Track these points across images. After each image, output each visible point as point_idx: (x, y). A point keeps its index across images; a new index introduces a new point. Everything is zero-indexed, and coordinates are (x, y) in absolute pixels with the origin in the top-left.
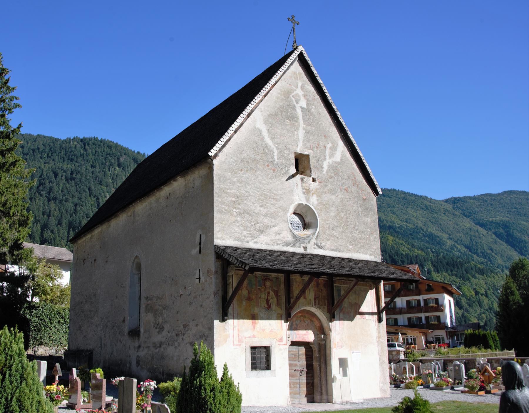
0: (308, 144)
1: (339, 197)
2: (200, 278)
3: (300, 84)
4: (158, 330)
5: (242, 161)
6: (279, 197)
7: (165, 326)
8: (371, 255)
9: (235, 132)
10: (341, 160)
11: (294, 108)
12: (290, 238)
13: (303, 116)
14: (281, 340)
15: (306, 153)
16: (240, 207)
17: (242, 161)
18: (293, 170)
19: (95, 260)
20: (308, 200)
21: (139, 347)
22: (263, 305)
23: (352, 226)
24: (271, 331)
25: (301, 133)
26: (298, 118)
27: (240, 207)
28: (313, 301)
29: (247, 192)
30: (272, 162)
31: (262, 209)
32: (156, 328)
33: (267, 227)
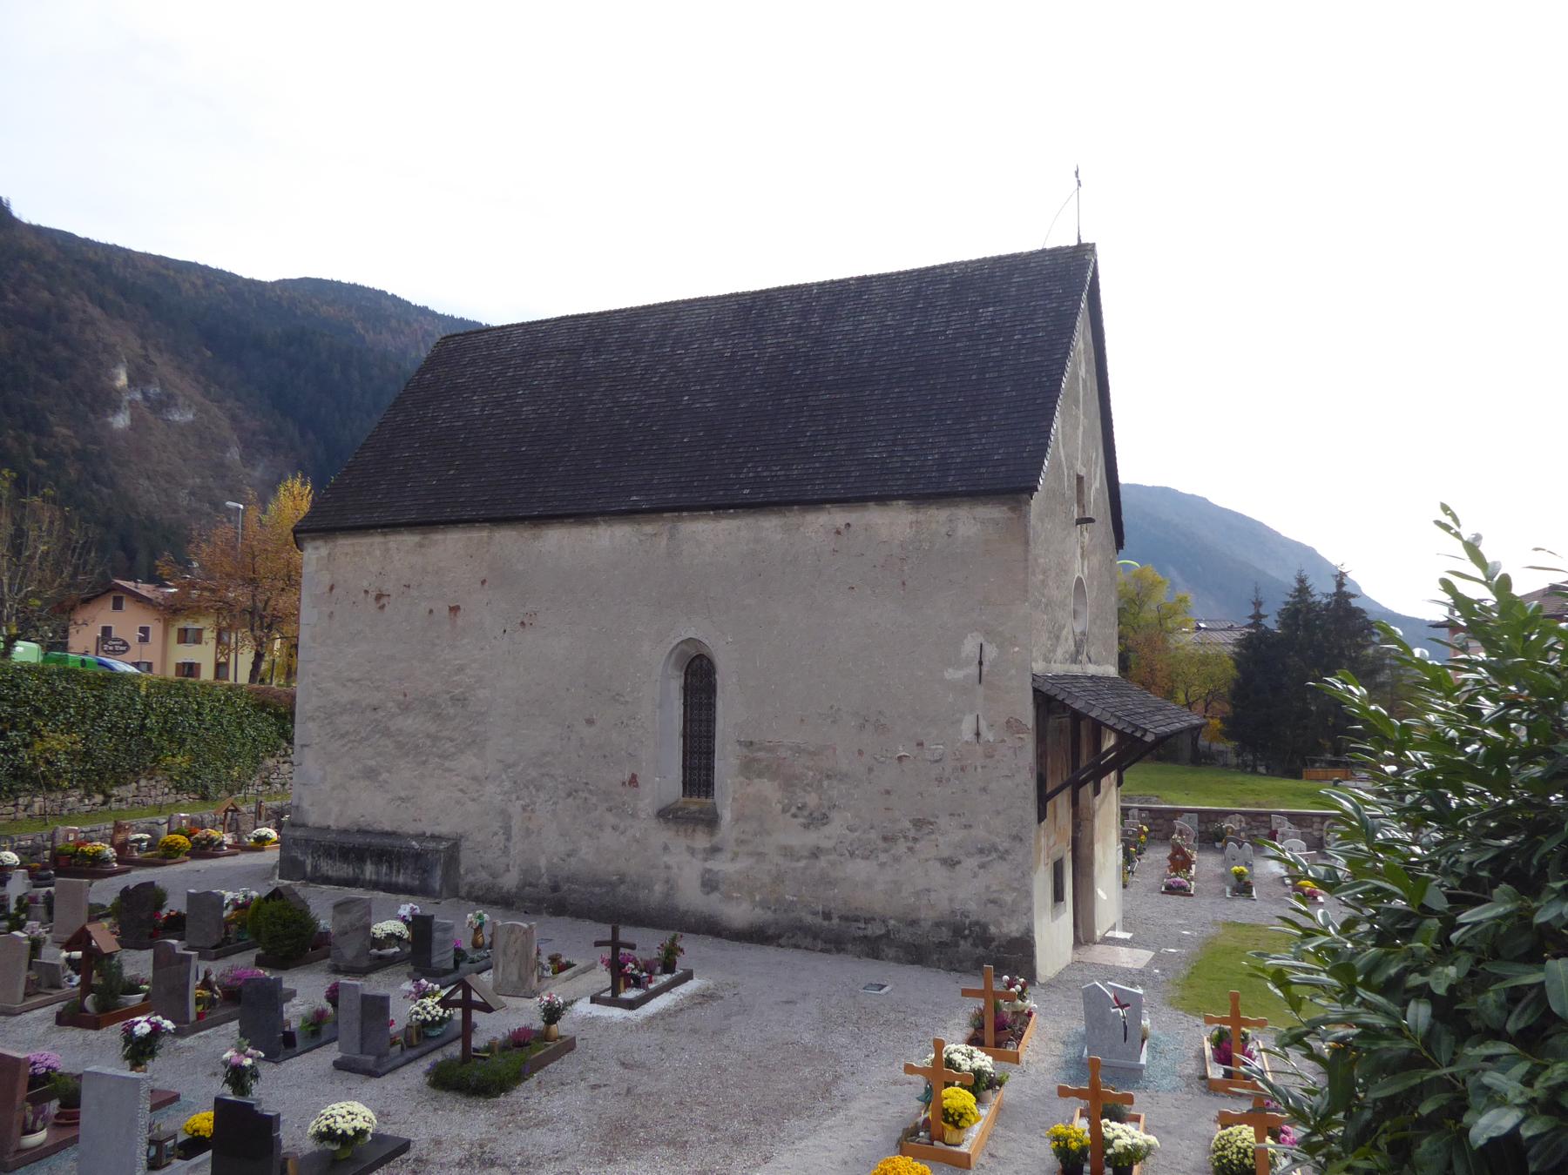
2: (978, 734)
4: (802, 820)
7: (833, 814)
19: (454, 610)
32: (794, 816)
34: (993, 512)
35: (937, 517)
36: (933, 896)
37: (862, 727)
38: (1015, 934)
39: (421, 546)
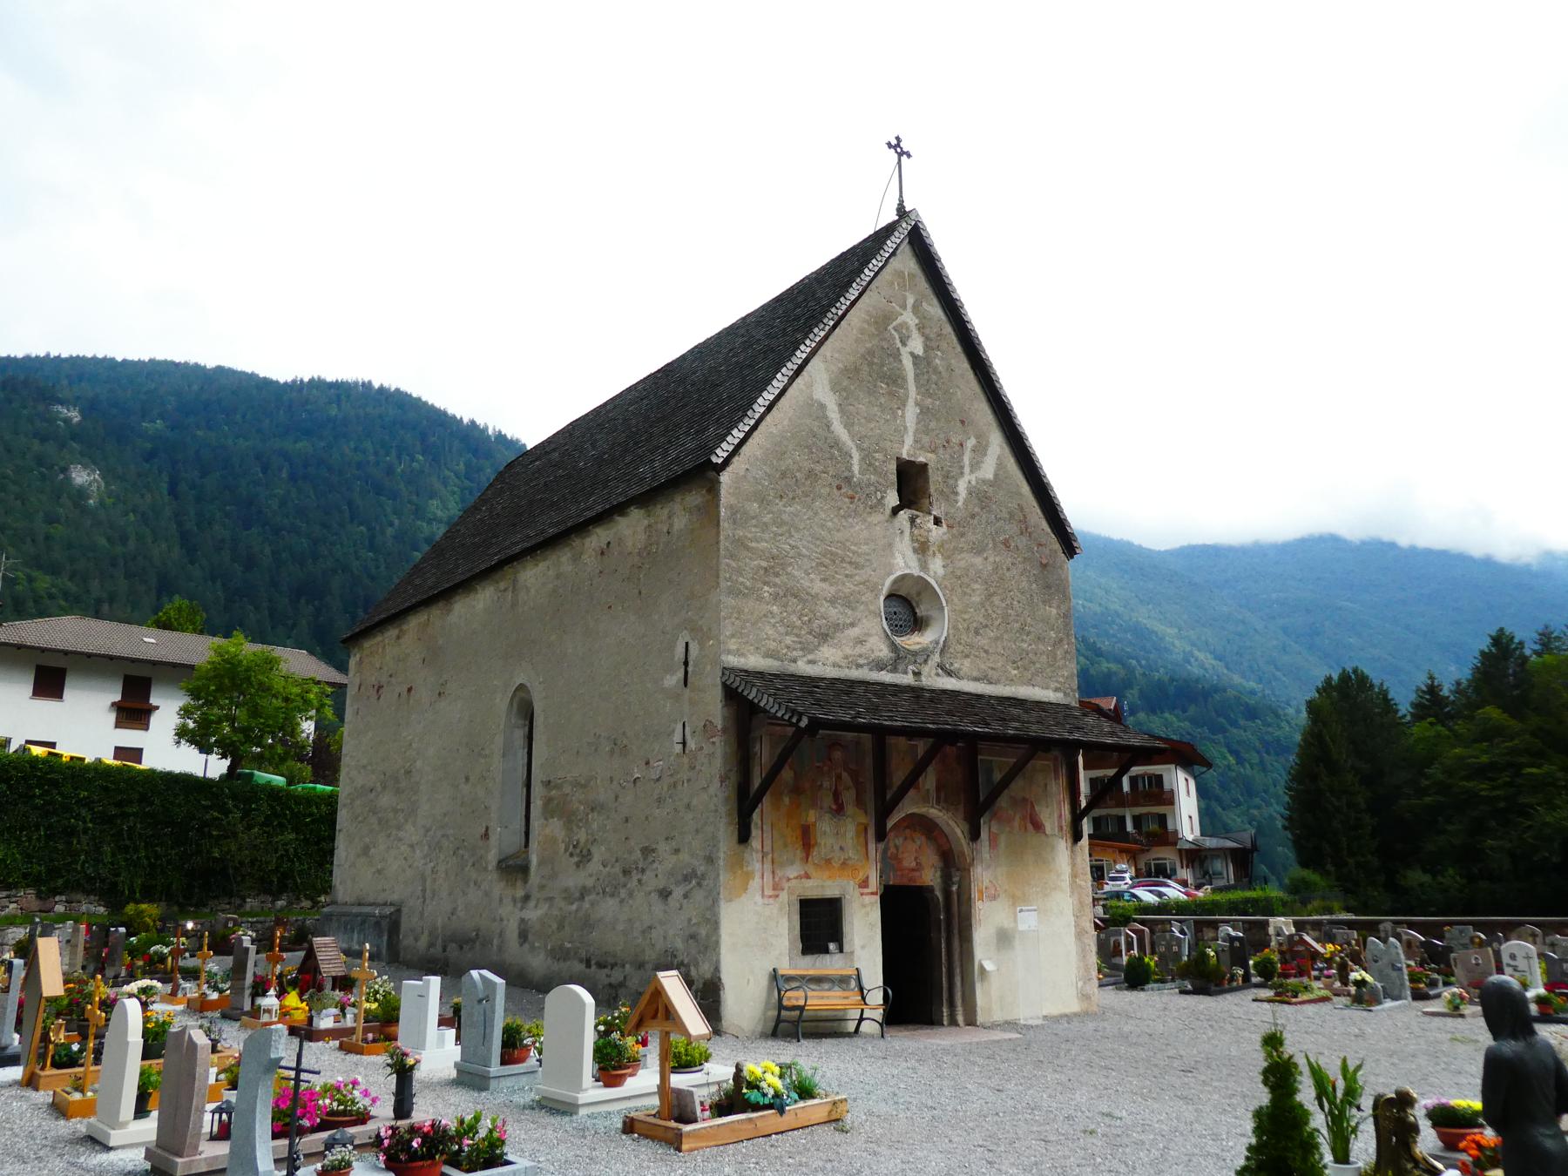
0: (926, 440)
1: (991, 559)
2: (684, 743)
3: (910, 301)
4: (576, 859)
5: (783, 475)
6: (861, 560)
7: (594, 850)
8: (1056, 690)
9: (769, 408)
10: (996, 475)
11: (897, 356)
12: (884, 652)
13: (916, 375)
14: (864, 884)
15: (922, 459)
16: (777, 580)
17: (783, 475)
18: (893, 499)
19: (410, 690)
20: (924, 566)
21: (527, 898)
23: (1017, 625)
25: (911, 413)
26: (904, 379)
27: (777, 580)
28: (933, 794)
29: (793, 547)
30: (848, 480)
31: (824, 585)
33: (837, 627)
34: (694, 498)
35: (661, 512)
36: (654, 934)
37: (612, 752)
38: (708, 976)
39: (398, 637)
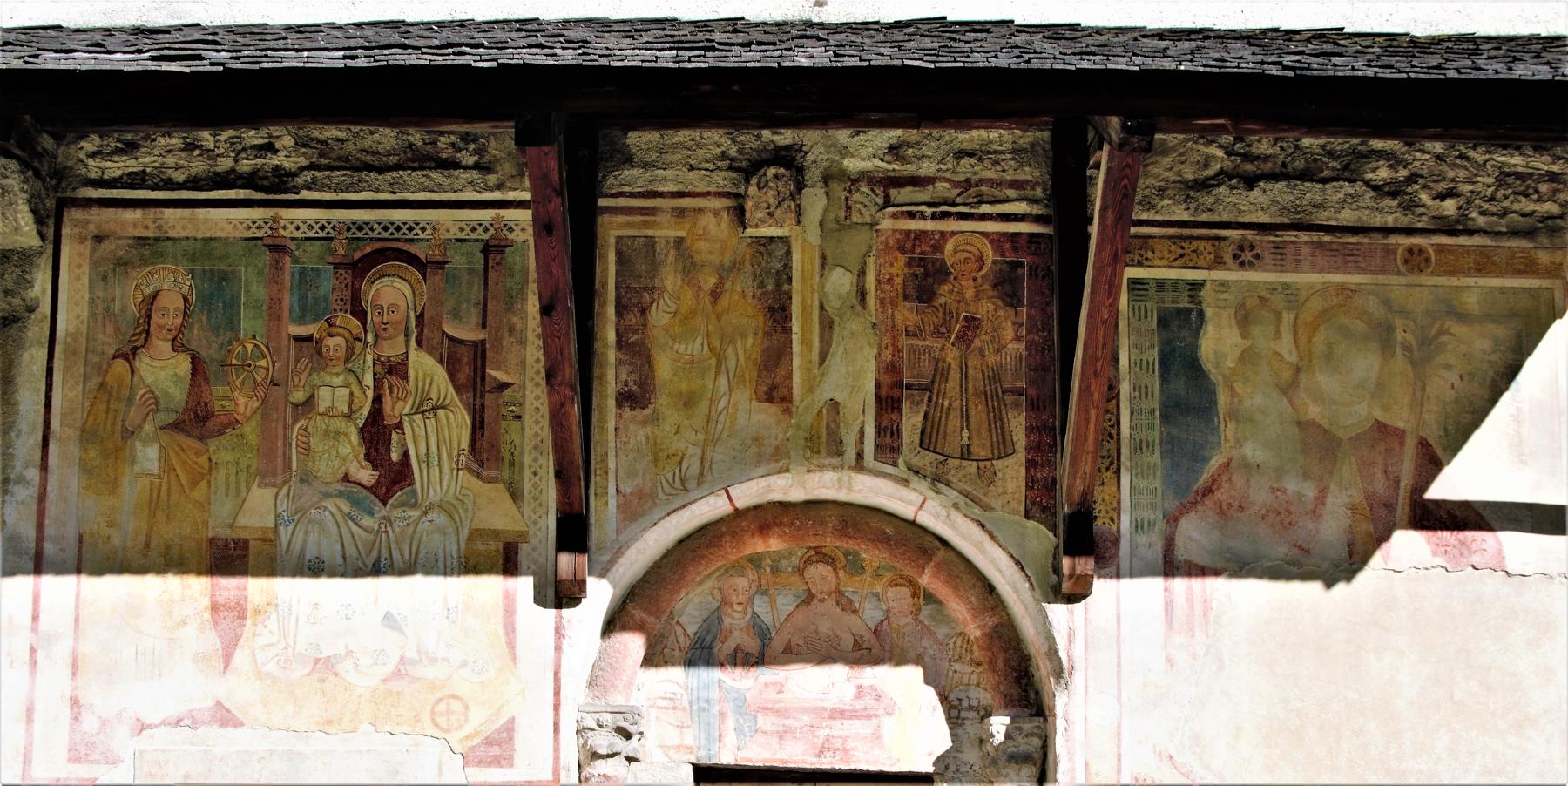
22: (327, 468)
24: (397, 674)
28: (861, 418)
